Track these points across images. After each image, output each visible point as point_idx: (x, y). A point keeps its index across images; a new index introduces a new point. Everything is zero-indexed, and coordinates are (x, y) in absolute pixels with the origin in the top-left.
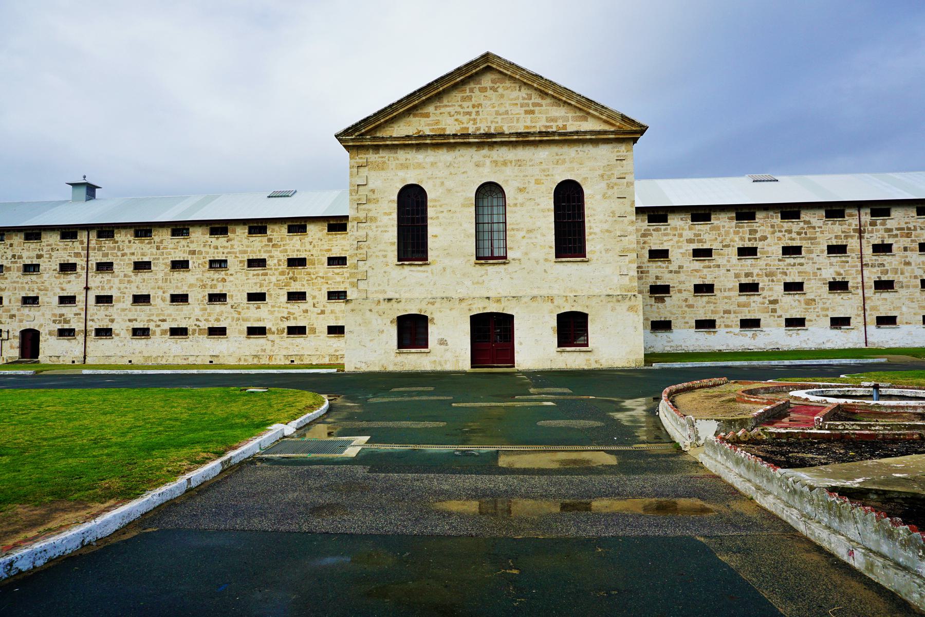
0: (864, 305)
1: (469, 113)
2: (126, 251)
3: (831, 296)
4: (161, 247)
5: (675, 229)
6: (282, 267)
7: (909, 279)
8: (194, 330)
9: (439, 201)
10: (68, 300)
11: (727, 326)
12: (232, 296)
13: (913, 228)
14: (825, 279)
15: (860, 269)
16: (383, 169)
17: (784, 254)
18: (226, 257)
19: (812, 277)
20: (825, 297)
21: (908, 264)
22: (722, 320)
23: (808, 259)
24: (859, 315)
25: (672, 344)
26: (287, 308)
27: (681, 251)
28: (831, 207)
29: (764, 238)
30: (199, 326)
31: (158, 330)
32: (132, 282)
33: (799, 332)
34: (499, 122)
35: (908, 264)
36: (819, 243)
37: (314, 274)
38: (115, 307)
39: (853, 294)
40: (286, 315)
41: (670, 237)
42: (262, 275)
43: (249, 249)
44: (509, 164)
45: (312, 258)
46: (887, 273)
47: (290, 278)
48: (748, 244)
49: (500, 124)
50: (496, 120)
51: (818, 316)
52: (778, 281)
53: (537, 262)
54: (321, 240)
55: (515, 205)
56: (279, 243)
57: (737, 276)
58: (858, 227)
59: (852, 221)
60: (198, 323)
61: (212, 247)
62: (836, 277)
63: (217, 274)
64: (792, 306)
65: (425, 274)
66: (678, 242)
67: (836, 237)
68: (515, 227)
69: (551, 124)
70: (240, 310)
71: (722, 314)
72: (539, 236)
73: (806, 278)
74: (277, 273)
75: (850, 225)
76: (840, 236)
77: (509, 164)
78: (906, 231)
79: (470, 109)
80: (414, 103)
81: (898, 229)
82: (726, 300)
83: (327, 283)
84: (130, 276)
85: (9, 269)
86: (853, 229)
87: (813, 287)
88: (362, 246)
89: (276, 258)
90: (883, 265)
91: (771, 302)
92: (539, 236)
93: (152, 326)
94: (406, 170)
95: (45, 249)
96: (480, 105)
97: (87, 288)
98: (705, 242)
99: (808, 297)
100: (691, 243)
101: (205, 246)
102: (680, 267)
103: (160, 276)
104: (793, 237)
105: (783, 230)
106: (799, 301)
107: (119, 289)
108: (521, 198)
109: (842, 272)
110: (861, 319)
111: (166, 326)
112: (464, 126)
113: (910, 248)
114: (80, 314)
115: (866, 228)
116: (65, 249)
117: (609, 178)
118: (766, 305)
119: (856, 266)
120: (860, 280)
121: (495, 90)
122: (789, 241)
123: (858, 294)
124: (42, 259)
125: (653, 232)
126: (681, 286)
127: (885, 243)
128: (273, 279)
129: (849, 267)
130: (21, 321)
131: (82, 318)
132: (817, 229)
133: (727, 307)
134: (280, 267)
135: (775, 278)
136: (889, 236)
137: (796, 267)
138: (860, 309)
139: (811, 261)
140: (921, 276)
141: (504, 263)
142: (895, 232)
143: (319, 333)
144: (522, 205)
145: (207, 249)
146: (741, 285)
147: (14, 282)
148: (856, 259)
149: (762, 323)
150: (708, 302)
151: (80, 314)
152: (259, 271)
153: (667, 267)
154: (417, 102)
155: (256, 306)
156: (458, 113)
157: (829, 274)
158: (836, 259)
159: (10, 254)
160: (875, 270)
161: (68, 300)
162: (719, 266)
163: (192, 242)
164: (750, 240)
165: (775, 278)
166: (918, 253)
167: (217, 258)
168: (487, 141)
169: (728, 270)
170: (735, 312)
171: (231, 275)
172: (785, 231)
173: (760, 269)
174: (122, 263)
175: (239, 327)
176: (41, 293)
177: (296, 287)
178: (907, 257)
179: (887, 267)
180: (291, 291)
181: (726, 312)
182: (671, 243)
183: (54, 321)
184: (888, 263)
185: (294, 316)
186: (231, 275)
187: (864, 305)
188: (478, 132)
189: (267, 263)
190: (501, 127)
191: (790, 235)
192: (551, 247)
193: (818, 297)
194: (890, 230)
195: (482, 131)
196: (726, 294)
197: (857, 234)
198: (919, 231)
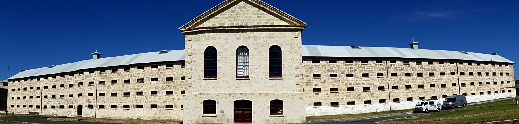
1: (234, 17)
4: (121, 75)
5: (323, 66)
6: (164, 81)
8: (132, 106)
9: (222, 53)
10: (91, 95)
11: (343, 104)
12: (145, 92)
14: (377, 86)
16: (199, 40)
17: (363, 76)
18: (143, 78)
21: (402, 80)
22: (341, 102)
23: (371, 78)
24: (388, 99)
25: (322, 112)
26: (166, 97)
27: (325, 74)
29: (356, 70)
30: (133, 104)
31: (119, 106)
32: (111, 88)
34: (247, 21)
35: (402, 80)
36: (374, 72)
37: (176, 84)
38: (105, 97)
39: (386, 91)
40: (165, 100)
41: (321, 69)
42: (156, 84)
43: (152, 74)
44: (250, 38)
45: (175, 77)
47: (167, 85)
48: (350, 73)
49: (247, 22)
50: (245, 20)
51: (375, 99)
52: (361, 86)
53: (262, 79)
54: (179, 70)
55: (253, 55)
56: (163, 72)
57: (346, 85)
59: (384, 63)
60: (133, 103)
61: (138, 74)
63: (140, 84)
64: (366, 96)
65: (216, 83)
66: (324, 71)
67: (380, 70)
68: (252, 64)
69: (268, 22)
70: (148, 98)
71: (341, 100)
72: (263, 68)
74: (162, 83)
75: (384, 66)
76: (381, 70)
77: (250, 38)
78: (401, 69)
79: (235, 16)
80: (212, 13)
81: (398, 68)
82: (342, 94)
83: (181, 87)
84: (110, 86)
86: (385, 67)
88: (190, 73)
89: (162, 78)
90: (394, 80)
91: (359, 95)
92: (263, 68)
93: (117, 105)
94: (208, 41)
96: (238, 14)
97: (97, 91)
98: (334, 71)
99: (371, 93)
100: (329, 71)
101: (135, 73)
102: (325, 81)
103: (120, 86)
105: (362, 67)
106: (368, 94)
107: (107, 90)
108: (255, 52)
109: (382, 83)
111: (122, 104)
112: (232, 23)
114: (94, 100)
117: (292, 44)
118: (357, 96)
119: (386, 81)
121: (245, 8)
122: (364, 72)
125: (314, 67)
126: (325, 88)
128: (160, 86)
131: (95, 101)
132: (373, 67)
133: (342, 97)
134: (163, 81)
135: (360, 86)
136: (396, 70)
141: (248, 79)
142: (398, 69)
143: (178, 107)
144: (256, 55)
145: (136, 75)
146: (348, 88)
148: (386, 78)
149: (355, 103)
150: (335, 95)
151: (94, 100)
152: (155, 82)
153: (320, 81)
154: (213, 13)
155: (154, 96)
156: (230, 17)
157: (378, 84)
158: (380, 78)
160: (392, 82)
161: (91, 95)
162: (339, 81)
163: (131, 72)
164: (351, 71)
165: (360, 86)
167: (140, 78)
168: (241, 29)
169: (343, 82)
170: (345, 99)
171: (145, 84)
172: (363, 68)
173: (355, 82)
174: (108, 81)
175: (148, 105)
176: (83, 92)
177: (169, 89)
178: (401, 78)
179: (396, 81)
180: (167, 90)
181: (342, 99)
182: (321, 71)
183: (87, 102)
185: (168, 101)
186: (145, 84)
188: (238, 25)
189: (158, 79)
190: (247, 23)
192: (268, 73)
194: (396, 68)
195: (239, 25)
196: (342, 92)
197: (386, 69)
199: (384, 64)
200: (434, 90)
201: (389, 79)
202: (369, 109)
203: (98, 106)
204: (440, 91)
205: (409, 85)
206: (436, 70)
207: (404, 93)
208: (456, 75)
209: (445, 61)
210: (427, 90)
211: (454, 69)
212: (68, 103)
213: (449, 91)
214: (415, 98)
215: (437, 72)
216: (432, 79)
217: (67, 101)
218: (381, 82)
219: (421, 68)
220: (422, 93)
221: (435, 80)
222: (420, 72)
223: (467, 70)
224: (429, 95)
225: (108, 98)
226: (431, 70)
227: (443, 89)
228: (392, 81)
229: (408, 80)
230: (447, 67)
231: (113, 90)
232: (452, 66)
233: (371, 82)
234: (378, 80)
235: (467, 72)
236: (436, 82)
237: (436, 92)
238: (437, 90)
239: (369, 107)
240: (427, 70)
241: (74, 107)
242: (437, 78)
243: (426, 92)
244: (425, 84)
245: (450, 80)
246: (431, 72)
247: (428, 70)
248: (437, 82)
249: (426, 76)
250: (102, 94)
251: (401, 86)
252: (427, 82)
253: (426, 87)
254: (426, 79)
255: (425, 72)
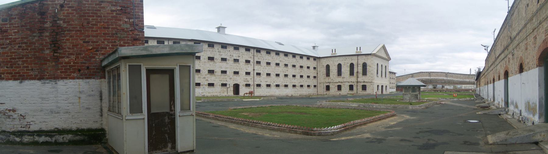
2: (264, 58)
4: (273, 58)
40: (300, 82)
43: (293, 62)
85: (229, 60)
93: (271, 84)
95: (241, 54)
97: (254, 70)
107: (263, 71)
111: (275, 84)
116: (247, 55)
124: (240, 58)
130: (233, 80)
147: (231, 65)
159: (229, 54)
161: (248, 74)
163: (280, 58)
174: (263, 62)
176: (240, 70)
183: (244, 81)
203: (255, 85)
212: (220, 80)
217: (220, 78)
225: (264, 78)
231: (268, 71)
241: (228, 86)
250: (259, 74)
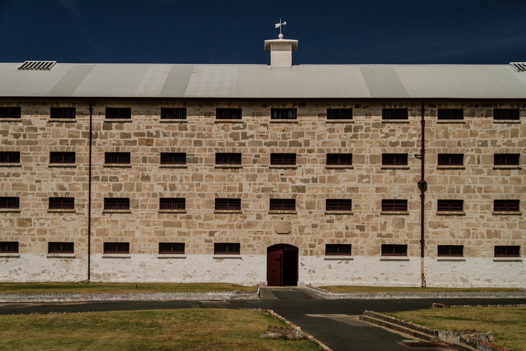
0: (89, 228)
3: (51, 216)
7: (146, 197)
13: (154, 134)
14: (45, 195)
15: (87, 182)
19: (29, 192)
20: (44, 217)
21: (146, 178)
23: (26, 168)
28: (58, 104)
33: (9, 259)
35: (146, 178)
36: (39, 149)
39: (78, 214)
46: (120, 188)
51: (33, 240)
58: (89, 131)
62: (58, 192)
67: (62, 142)
73: (22, 192)
76: (67, 141)
78: (146, 138)
81: (136, 134)
86: (83, 133)
87: (29, 204)
99: (22, 217)
104: (9, 140)
106: (11, 221)
109: (66, 185)
110: (85, 246)
113: (149, 158)
115: (99, 132)
119: (84, 179)
120: (86, 197)
123: (83, 214)
127: (120, 151)
129: (74, 179)
132: (39, 131)
136: (126, 143)
137: (11, 178)
138: (84, 232)
139: (29, 172)
140: (161, 194)
142: (133, 138)
148: (84, 171)
160: (105, 184)
166: (159, 165)
178: (145, 169)
179: (121, 181)
184: (122, 176)
187: (89, 228)
191: (6, 138)
193: (34, 217)
194: (128, 135)
197: (87, 140)
198: (162, 138)
199: (80, 122)
200: (285, 219)
201: (96, 173)
202: (11, 272)
204: (314, 226)
205: (175, 197)
206: (307, 143)
207: (149, 225)
208: (414, 164)
209: (357, 106)
210: (252, 218)
211: (406, 139)
213: (361, 228)
214: (197, 246)
215: (310, 151)
216: (284, 180)
218: (61, 182)
219: (235, 137)
220: (227, 230)
221: (299, 184)
222: (228, 150)
223: (485, 144)
224: (259, 238)
226: (283, 144)
227: (330, 221)
228: (104, 179)
229: (174, 178)
230: (367, 130)
232: (392, 126)
233: (25, 182)
234: (53, 176)
235: (479, 151)
236: (302, 189)
237: (295, 228)
238: (303, 221)
239: (8, 263)
240: (263, 141)
242: (305, 177)
243: (249, 225)
244: (246, 195)
245: (376, 185)
246: (279, 150)
247: (268, 144)
248: (308, 192)
249: (256, 166)
251: (142, 198)
252: (255, 191)
253: (251, 208)
254: (254, 178)
255: (253, 151)
